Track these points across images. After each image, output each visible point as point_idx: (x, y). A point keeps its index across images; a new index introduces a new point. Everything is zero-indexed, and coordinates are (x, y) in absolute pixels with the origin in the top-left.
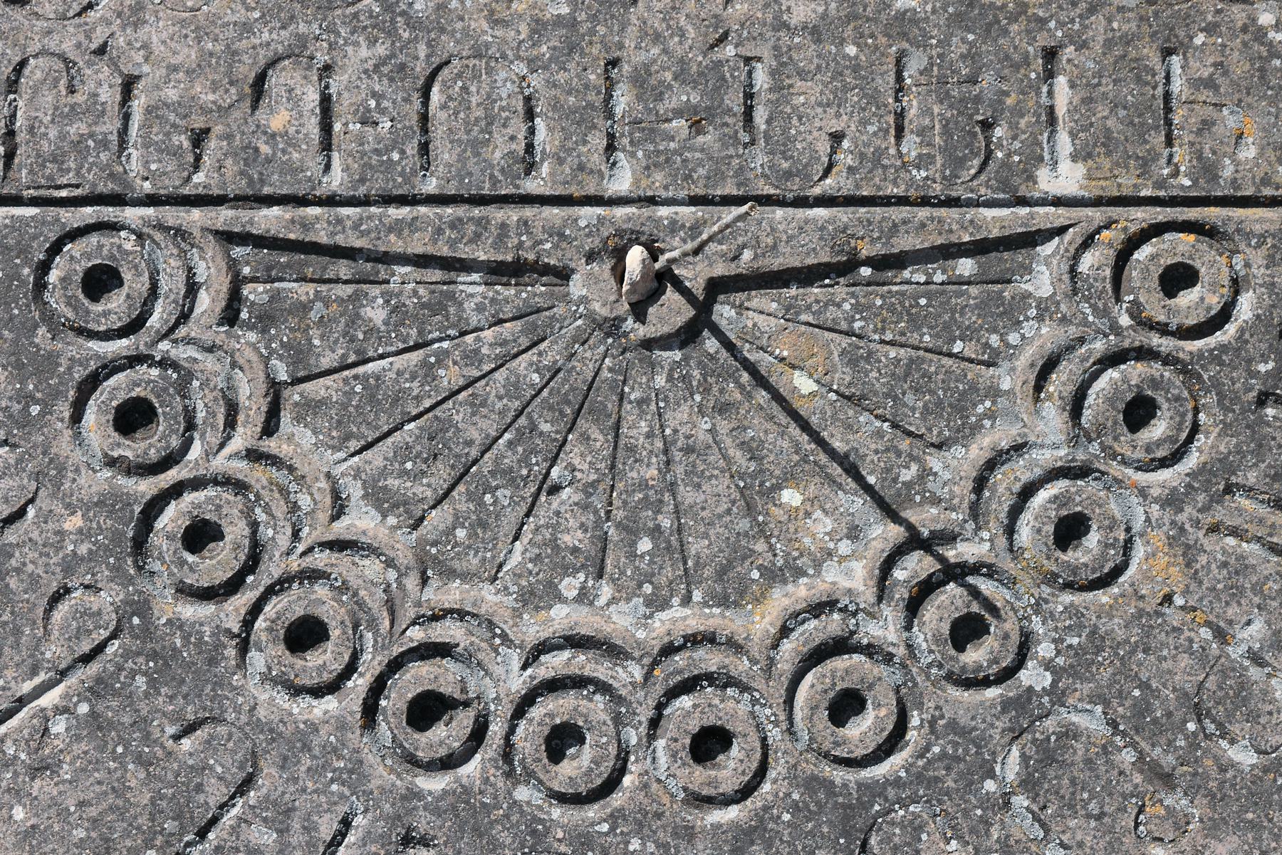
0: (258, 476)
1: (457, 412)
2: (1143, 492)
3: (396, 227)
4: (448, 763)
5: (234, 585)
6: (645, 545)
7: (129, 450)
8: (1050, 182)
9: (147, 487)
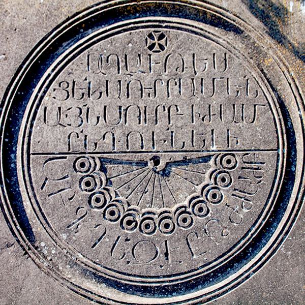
3: (124, 156)
4: (132, 229)
7: (88, 188)
8: (212, 149)
9: (90, 193)
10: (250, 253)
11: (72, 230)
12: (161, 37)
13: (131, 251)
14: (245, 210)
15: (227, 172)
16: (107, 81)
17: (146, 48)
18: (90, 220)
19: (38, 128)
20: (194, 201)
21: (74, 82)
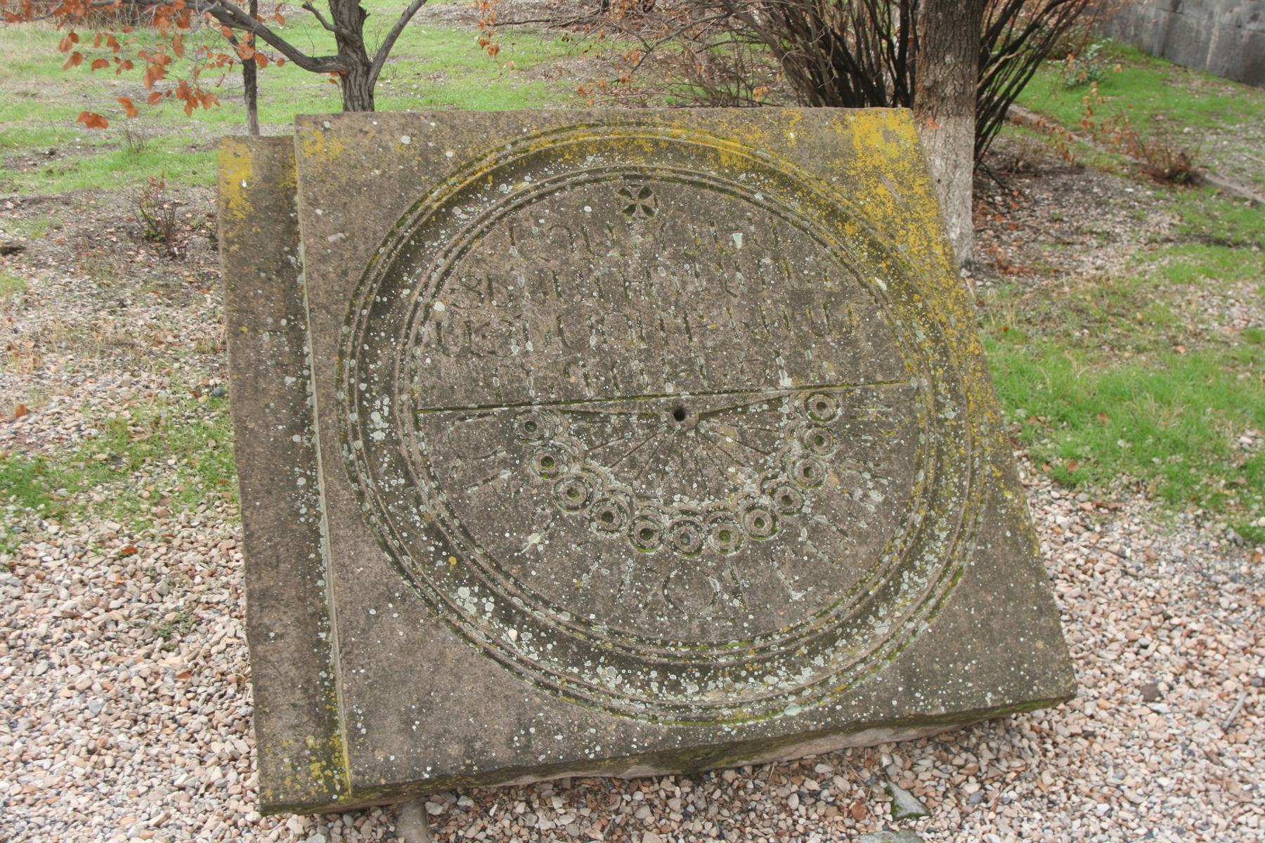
0: (585, 474)
5: (584, 506)
6: (695, 485)
7: (547, 470)
12: (645, 193)
14: (877, 497)
19: (428, 361)
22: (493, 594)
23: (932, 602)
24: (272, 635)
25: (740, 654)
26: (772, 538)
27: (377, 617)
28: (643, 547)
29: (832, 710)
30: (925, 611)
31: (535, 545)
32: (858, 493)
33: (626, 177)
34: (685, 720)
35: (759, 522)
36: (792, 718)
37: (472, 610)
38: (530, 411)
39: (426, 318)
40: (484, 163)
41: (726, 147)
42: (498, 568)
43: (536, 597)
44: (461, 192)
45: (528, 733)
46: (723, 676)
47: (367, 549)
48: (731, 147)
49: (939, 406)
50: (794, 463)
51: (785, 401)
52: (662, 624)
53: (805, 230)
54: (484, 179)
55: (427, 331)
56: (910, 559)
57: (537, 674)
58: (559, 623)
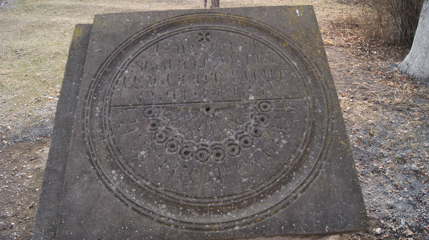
0: (167, 130)
1: (188, 123)
2: (263, 127)
5: (164, 141)
6: (210, 135)
7: (153, 128)
9: (155, 132)
10: (295, 177)
11: (139, 159)
12: (208, 34)
13: (188, 176)
14: (284, 142)
15: (265, 114)
16: (170, 60)
17: (197, 40)
18: (154, 151)
19: (119, 89)
20: (239, 136)
21: (146, 62)
22: (124, 173)
23: (305, 185)
24: (50, 183)
25: (217, 202)
26: (237, 156)
27: (78, 179)
28: (184, 158)
29: (254, 229)
30: (301, 189)
31: (143, 155)
32: (276, 140)
33: (201, 29)
34: (190, 229)
35: (233, 150)
36: (236, 231)
37: (115, 178)
38: (151, 107)
39: (121, 75)
40: (153, 26)
41: (240, 19)
42: (127, 163)
43: (139, 175)
44: (144, 35)
45: (125, 227)
46: (210, 211)
47: (81, 154)
48: (242, 19)
49: (315, 108)
50: (251, 128)
51: (251, 104)
52: (187, 188)
53: (266, 45)
54: (152, 31)
55: (121, 79)
56: (297, 168)
57: (133, 205)
58: (146, 186)
